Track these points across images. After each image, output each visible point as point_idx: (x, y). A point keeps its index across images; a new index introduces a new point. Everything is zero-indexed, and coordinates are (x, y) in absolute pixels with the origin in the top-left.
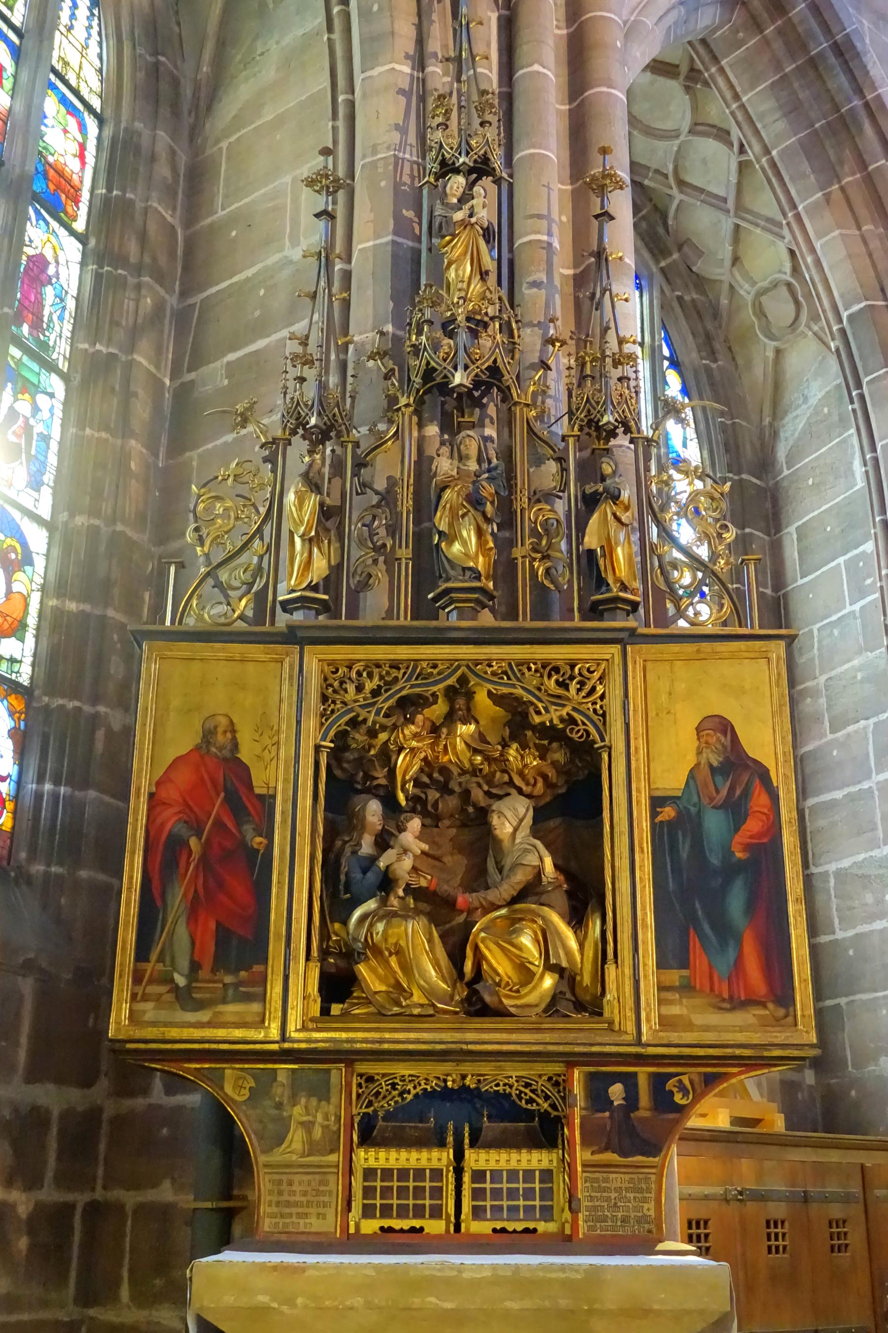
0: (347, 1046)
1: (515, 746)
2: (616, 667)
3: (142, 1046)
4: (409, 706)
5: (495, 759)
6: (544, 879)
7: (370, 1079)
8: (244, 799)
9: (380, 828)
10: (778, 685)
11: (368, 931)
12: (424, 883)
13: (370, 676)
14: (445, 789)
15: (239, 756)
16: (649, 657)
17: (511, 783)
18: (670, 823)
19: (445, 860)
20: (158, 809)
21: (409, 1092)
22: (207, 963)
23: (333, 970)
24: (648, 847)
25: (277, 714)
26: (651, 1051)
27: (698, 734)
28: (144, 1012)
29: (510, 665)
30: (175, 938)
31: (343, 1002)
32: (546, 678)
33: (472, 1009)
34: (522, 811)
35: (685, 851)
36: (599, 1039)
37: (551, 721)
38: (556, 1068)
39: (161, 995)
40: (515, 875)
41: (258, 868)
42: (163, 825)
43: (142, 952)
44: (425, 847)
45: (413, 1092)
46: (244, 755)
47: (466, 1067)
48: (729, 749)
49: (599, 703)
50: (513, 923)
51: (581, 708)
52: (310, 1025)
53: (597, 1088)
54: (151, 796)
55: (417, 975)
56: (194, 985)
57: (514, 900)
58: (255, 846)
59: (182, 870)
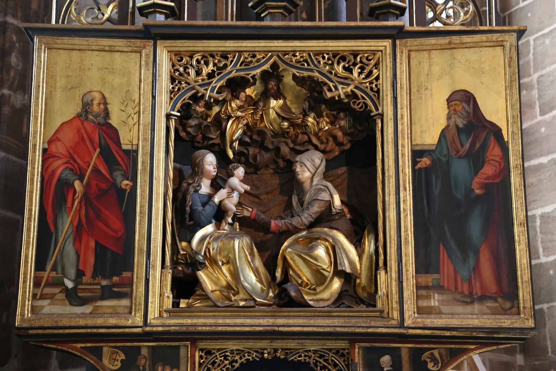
0: (192, 329)
1: (313, 115)
2: (388, 57)
3: (41, 332)
4: (236, 86)
5: (298, 125)
6: (334, 210)
7: (209, 352)
8: (114, 152)
9: (215, 174)
10: (510, 67)
11: (207, 247)
12: (246, 214)
13: (207, 64)
14: (262, 146)
15: (110, 121)
16: (412, 48)
17: (310, 142)
18: (426, 169)
19: (262, 197)
20: (51, 160)
21: (236, 362)
22: (89, 271)
23: (181, 275)
24: (409, 187)
25: (137, 90)
26: (411, 331)
27: (448, 104)
28: (42, 307)
29: (309, 54)
30: (64, 252)
31: (188, 298)
32: (335, 65)
33: (282, 302)
34: (318, 162)
35: (436, 190)
36: (373, 324)
37: (339, 96)
38: (341, 344)
39: (55, 294)
40: (312, 206)
41: (125, 204)
42: (54, 172)
43: (40, 265)
44: (248, 188)
45: (239, 361)
46: (114, 121)
47: (278, 344)
48: (471, 115)
49: (375, 83)
50: (311, 242)
51: (361, 87)
52: (165, 315)
54: (45, 151)
55: (242, 279)
56: (80, 287)
58: (123, 187)
59: (69, 205)
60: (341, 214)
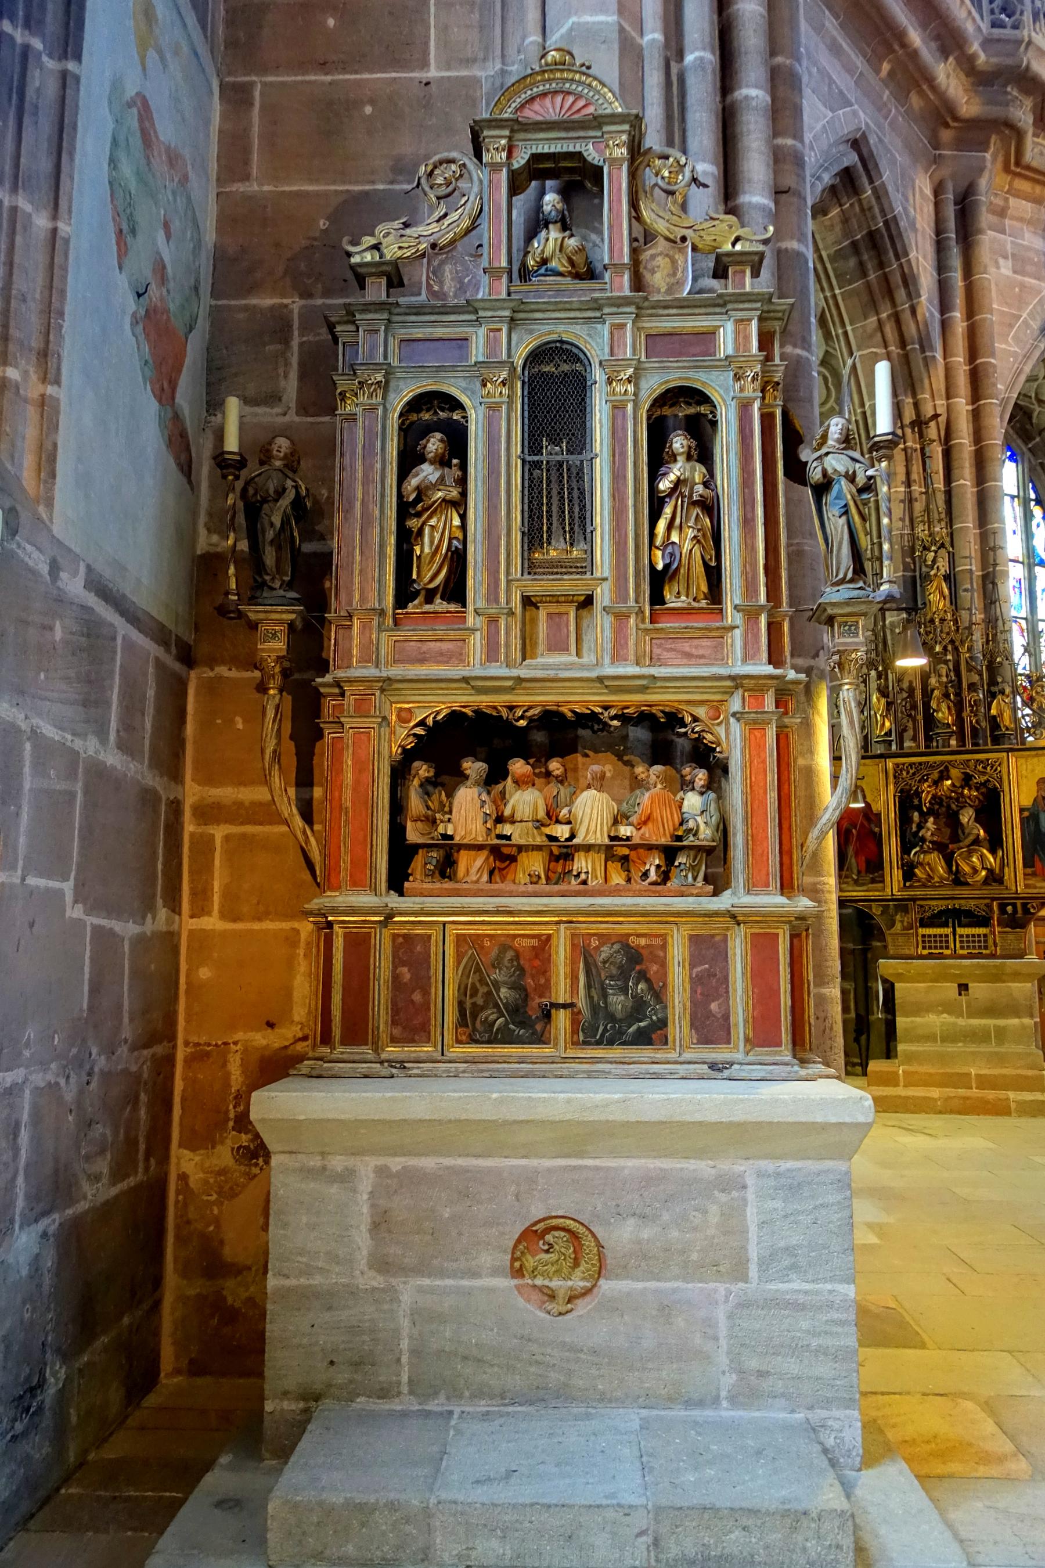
14: (941, 805)
38: (987, 901)
41: (878, 840)
50: (970, 853)
53: (1002, 908)
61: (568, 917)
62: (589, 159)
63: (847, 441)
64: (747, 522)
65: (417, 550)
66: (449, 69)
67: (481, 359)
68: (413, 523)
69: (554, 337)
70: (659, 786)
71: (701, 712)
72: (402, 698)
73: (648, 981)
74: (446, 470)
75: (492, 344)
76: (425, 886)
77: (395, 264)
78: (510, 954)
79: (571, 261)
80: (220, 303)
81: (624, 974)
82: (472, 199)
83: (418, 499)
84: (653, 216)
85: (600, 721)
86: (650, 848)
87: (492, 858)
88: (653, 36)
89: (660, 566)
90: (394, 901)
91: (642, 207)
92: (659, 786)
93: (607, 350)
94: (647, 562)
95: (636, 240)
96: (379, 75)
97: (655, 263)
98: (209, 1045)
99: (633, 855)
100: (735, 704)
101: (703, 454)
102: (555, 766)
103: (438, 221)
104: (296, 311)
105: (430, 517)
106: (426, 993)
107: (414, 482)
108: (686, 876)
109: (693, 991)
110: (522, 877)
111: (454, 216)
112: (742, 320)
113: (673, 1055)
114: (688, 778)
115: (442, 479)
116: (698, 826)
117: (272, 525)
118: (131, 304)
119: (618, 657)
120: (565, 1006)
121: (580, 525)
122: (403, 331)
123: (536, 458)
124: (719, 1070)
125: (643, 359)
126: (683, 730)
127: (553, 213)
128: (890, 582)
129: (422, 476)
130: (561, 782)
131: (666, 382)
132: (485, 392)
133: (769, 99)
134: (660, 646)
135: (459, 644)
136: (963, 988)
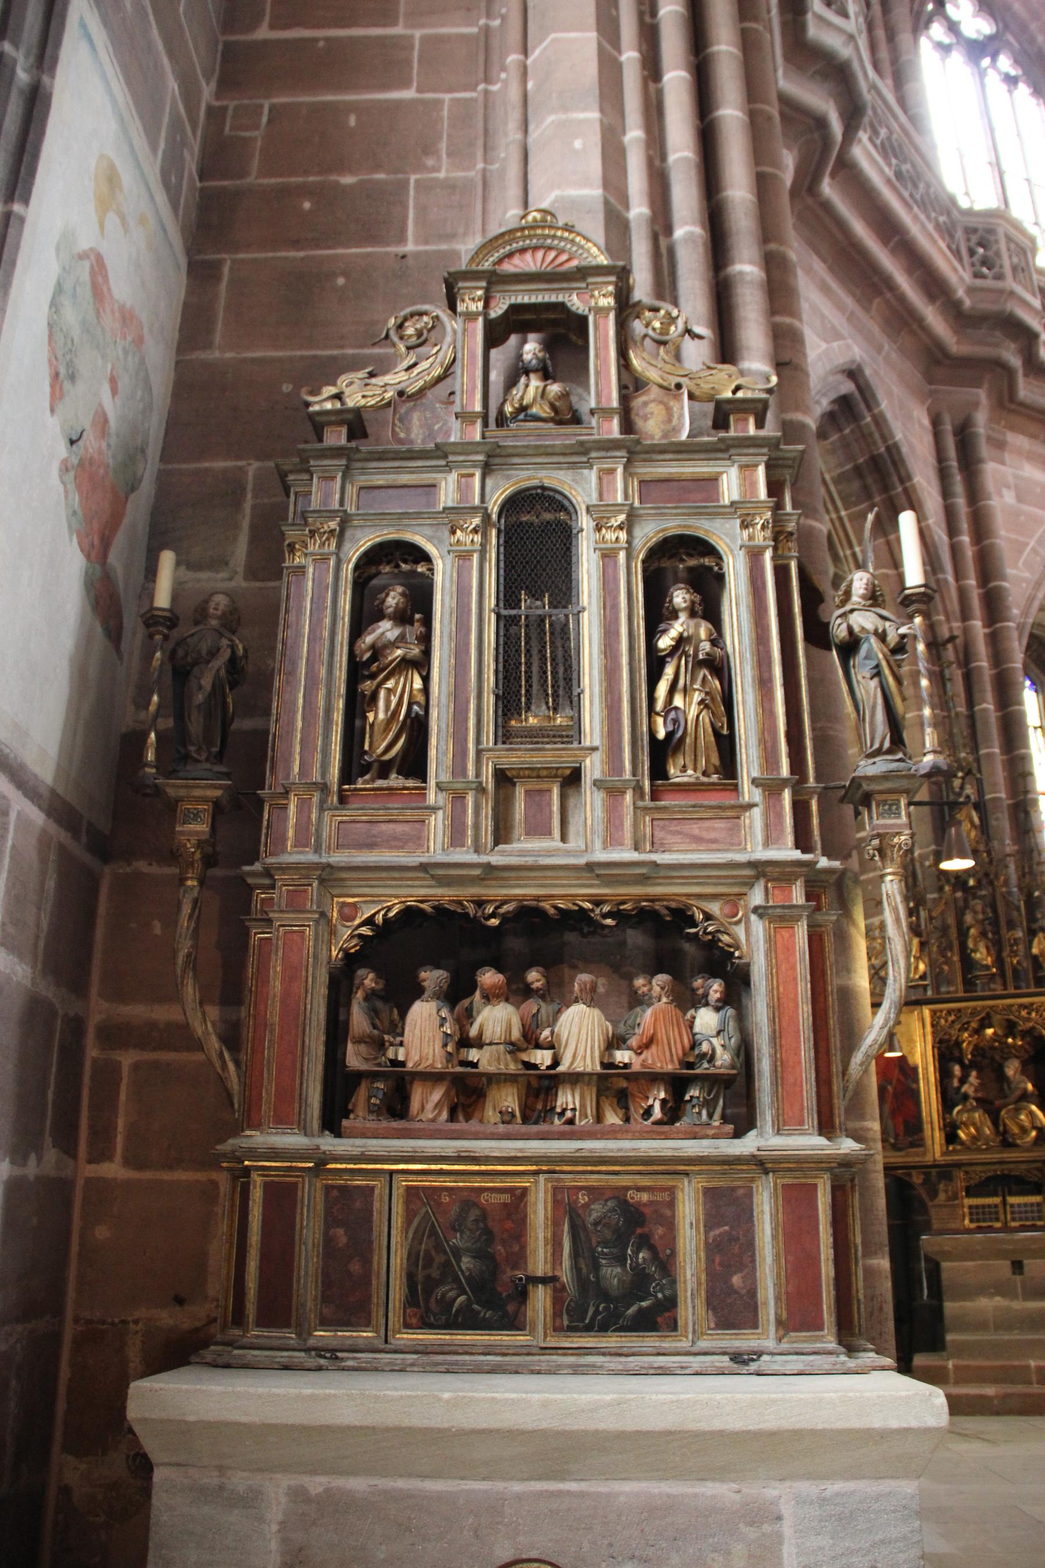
14: (983, 1056)
47: (1005, 1166)
50: (1018, 1111)
57: (1016, 1102)
60: (1033, 1094)
61: (549, 1164)
62: (574, 309)
63: (874, 598)
64: (764, 684)
65: (371, 716)
66: (426, 242)
67: (450, 504)
68: (367, 686)
69: (535, 482)
70: (664, 1000)
71: (715, 908)
72: (345, 891)
73: (652, 1248)
74: (408, 628)
75: (463, 490)
76: (368, 1125)
77: (357, 411)
78: (474, 1214)
79: (553, 407)
80: (170, 467)
81: (620, 1239)
82: (445, 348)
83: (374, 658)
84: (644, 364)
85: (591, 921)
86: (654, 1078)
87: (453, 1092)
88: (638, 210)
89: (661, 734)
90: (328, 1143)
91: (632, 354)
92: (664, 1000)
93: (595, 495)
94: (645, 729)
95: (626, 387)
96: (354, 250)
97: (648, 410)
98: (104, 1322)
99: (633, 1088)
100: (757, 897)
101: (709, 609)
102: (534, 977)
103: (407, 370)
104: (251, 474)
105: (387, 679)
106: (367, 1262)
107: (369, 639)
108: (699, 1113)
109: (710, 1260)
110: (491, 1114)
111: (424, 365)
112: (748, 466)
113: (684, 1344)
114: (701, 992)
115: (402, 638)
116: (714, 1050)
117: (200, 687)
118: (62, 450)
119: (611, 840)
120: (544, 1280)
121: (565, 689)
122: (362, 478)
123: (513, 612)
124: (745, 1363)
125: (637, 504)
126: (693, 930)
127: (534, 362)
128: (934, 752)
129: (379, 631)
130: (543, 997)
131: (663, 530)
132: (453, 539)
133: (763, 275)
134: (663, 828)
135: (418, 826)
136: (1018, 1267)
